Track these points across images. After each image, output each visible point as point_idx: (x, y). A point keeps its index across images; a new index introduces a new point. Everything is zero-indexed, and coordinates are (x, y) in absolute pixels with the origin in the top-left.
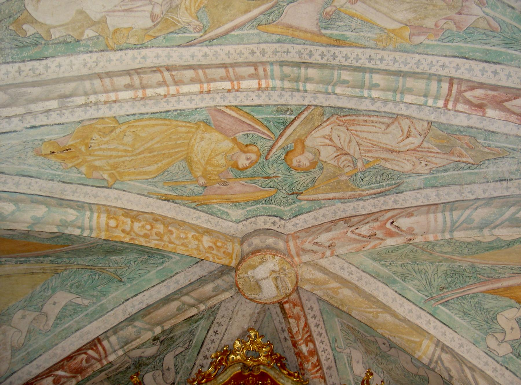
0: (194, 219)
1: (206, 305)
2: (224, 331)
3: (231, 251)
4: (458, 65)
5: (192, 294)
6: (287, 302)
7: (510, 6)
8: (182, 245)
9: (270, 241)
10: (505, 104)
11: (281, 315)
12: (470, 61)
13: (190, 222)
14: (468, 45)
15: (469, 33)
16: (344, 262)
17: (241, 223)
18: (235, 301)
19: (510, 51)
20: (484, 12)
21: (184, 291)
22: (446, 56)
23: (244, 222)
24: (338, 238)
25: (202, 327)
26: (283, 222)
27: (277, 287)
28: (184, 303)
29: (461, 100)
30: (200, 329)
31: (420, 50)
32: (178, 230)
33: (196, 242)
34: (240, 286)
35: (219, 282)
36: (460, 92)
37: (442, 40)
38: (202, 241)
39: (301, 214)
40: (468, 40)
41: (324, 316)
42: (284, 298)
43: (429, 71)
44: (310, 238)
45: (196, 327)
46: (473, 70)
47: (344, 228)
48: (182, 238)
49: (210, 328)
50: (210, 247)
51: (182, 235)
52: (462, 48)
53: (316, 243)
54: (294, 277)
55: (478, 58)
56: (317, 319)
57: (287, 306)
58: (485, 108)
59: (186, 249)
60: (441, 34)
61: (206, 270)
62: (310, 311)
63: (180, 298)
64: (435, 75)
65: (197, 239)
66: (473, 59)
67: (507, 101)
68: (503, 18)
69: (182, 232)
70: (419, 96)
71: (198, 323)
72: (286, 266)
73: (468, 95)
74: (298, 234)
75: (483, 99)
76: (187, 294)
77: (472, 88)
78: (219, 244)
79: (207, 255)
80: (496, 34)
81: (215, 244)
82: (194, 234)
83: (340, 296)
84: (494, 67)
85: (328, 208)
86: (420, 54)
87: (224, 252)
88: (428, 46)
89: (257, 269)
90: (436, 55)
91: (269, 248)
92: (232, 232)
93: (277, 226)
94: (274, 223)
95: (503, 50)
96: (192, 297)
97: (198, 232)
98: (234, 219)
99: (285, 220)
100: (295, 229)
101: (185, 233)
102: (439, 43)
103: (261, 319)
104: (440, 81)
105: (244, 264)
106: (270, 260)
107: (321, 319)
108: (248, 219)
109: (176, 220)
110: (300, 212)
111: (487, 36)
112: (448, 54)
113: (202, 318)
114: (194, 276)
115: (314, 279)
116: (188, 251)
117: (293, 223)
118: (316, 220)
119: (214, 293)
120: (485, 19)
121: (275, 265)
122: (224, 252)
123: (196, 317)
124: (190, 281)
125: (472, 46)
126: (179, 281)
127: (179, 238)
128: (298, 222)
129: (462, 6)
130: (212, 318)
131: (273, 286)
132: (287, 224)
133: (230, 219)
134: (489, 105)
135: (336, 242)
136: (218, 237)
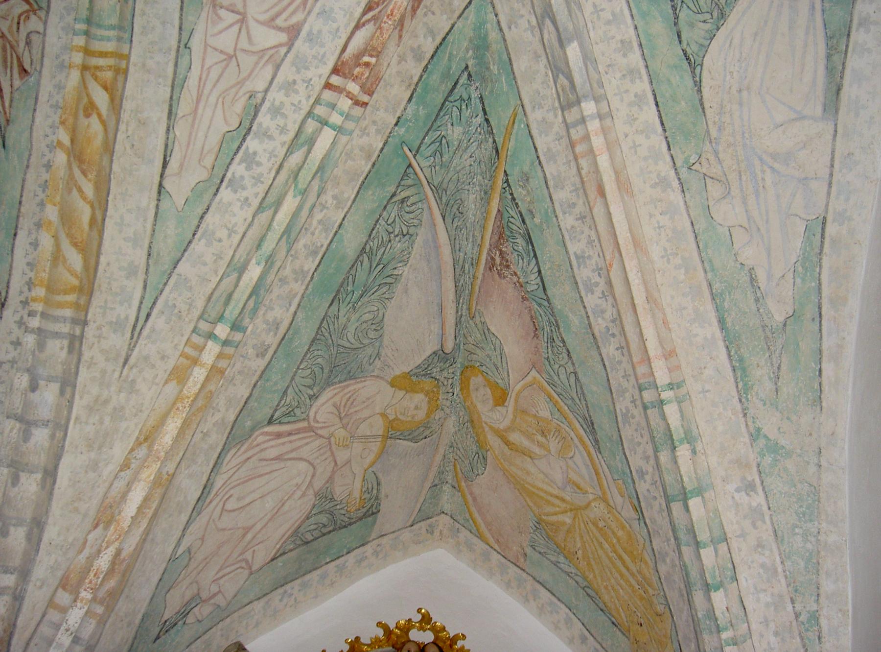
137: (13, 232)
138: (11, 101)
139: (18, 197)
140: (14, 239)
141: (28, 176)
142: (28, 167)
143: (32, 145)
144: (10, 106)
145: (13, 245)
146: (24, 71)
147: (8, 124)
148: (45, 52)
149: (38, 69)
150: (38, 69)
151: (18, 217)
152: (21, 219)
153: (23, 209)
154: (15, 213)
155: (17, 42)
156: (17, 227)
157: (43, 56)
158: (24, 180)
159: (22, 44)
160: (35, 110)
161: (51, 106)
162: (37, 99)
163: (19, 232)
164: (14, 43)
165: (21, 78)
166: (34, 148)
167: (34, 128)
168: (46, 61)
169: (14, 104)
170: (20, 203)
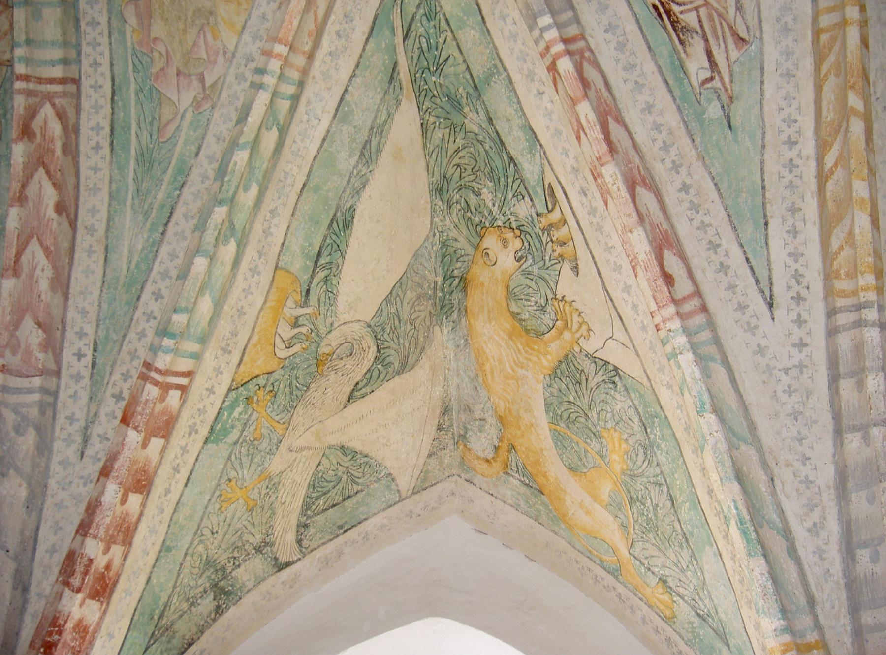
4: (101, 87)
7: (199, 148)
10: (41, 171)
12: (109, 106)
14: (133, 96)
15: (151, 94)
19: (132, 163)
20: (185, 111)
22: (112, 65)
29: (31, 101)
31: (115, 23)
36: (49, 97)
37: (134, 53)
40: (141, 96)
43: (84, 43)
46: (97, 112)
52: (128, 89)
55: (116, 116)
58: (25, 139)
60: (143, 50)
64: (79, 54)
66: (113, 109)
67: (48, 172)
68: (180, 143)
70: (27, 33)
73: (47, 111)
75: (43, 136)
77: (61, 115)
80: (155, 137)
84: (106, 144)
86: (109, 22)
88: (122, 33)
90: (111, 49)
95: (133, 152)
102: (130, 51)
104: (65, 62)
111: (151, 124)
112: (116, 68)
120: (176, 114)
125: (133, 103)
129: (190, 75)
134: (33, 147)
137: (762, 221)
138: (731, 75)
139: (760, 182)
140: (766, 230)
141: (766, 157)
142: (763, 147)
143: (763, 122)
144: (731, 82)
145: (767, 235)
146: (741, 41)
147: (732, 102)
148: (762, 16)
149: (758, 35)
150: (758, 35)
151: (764, 204)
152: (768, 206)
153: (767, 195)
154: (759, 200)
155: (725, 8)
156: (765, 216)
157: (760, 22)
158: (762, 163)
159: (732, 11)
160: (762, 82)
161: (781, 75)
162: (762, 69)
163: (770, 221)
164: (721, 10)
165: (739, 48)
166: (767, 125)
167: (765, 102)
168: (766, 27)
169: (736, 78)
170: (763, 188)
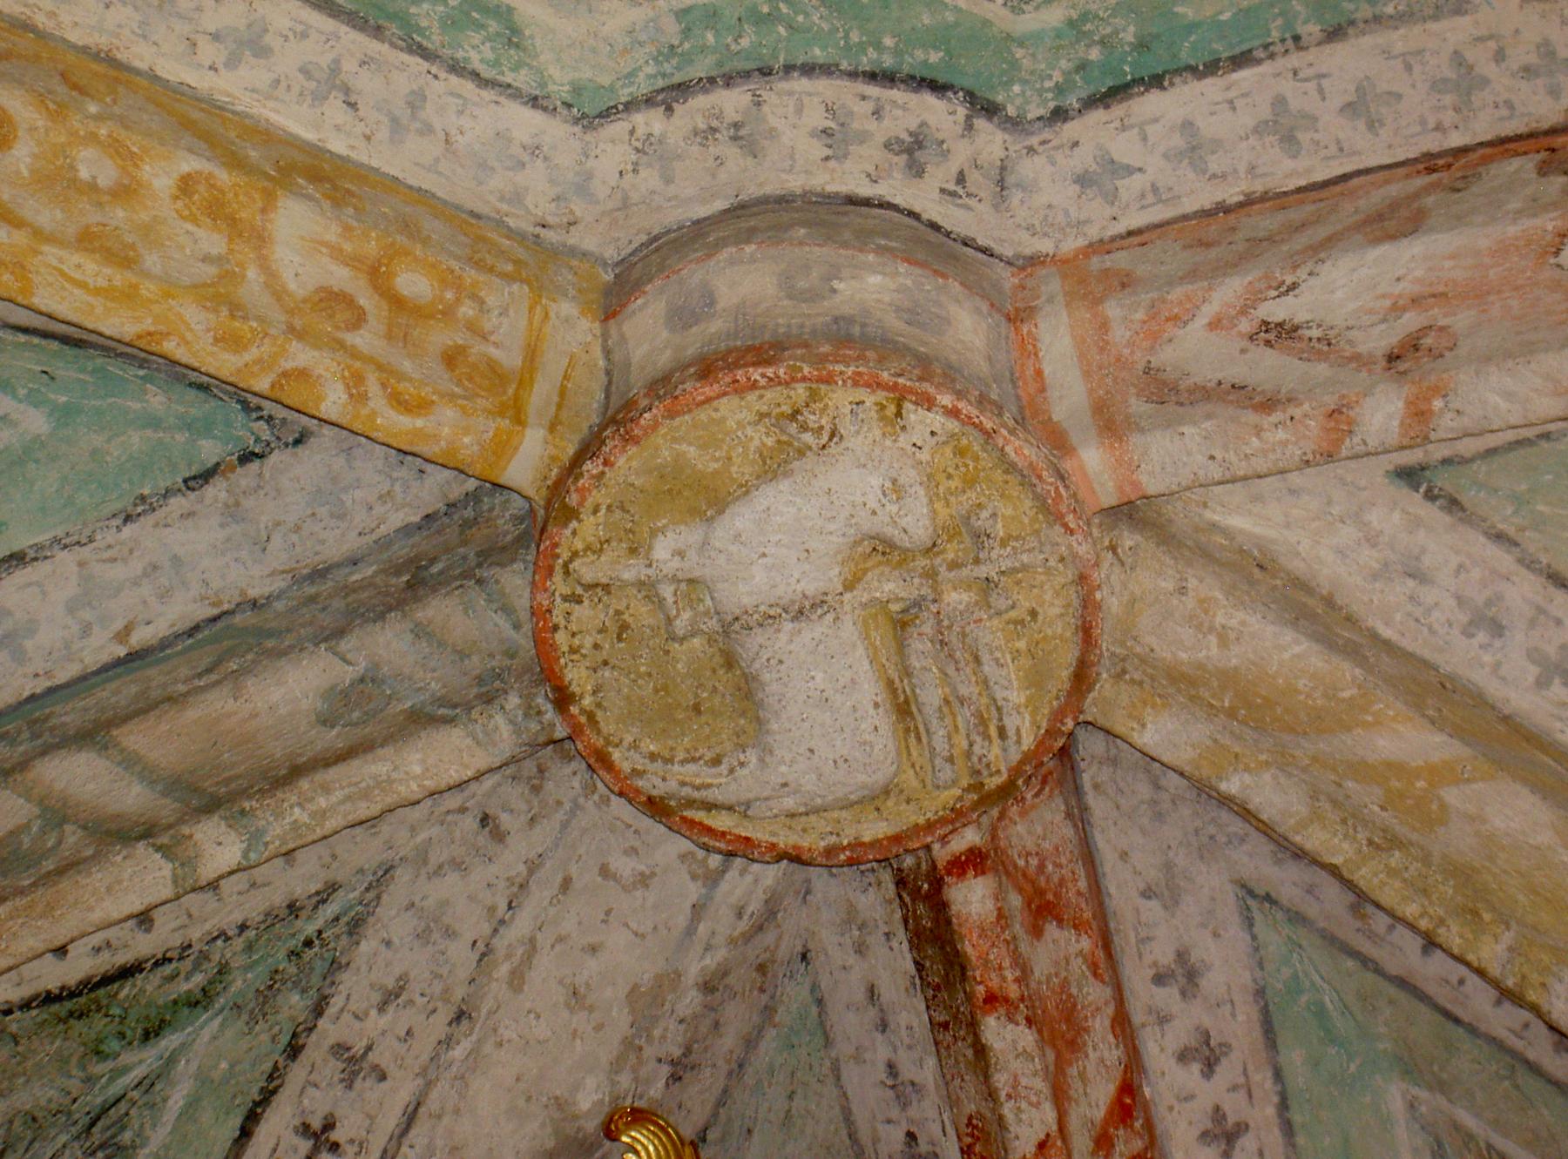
0: (209, 52)
1: (255, 837)
2: (390, 1121)
3: (510, 359)
5: (134, 738)
6: (972, 862)
8: (87, 240)
9: (873, 287)
11: (911, 1014)
13: (172, 70)
16: (1503, 559)
17: (618, 128)
18: (511, 859)
21: (70, 715)
23: (650, 122)
24: (1477, 294)
25: (202, 1078)
26: (991, 141)
27: (904, 710)
28: (56, 813)
30: (177, 1099)
32: (58, 114)
33: (213, 241)
34: (576, 676)
35: (387, 644)
38: (261, 240)
39: (1156, 81)
41: (1294, 1058)
42: (956, 817)
44: (1230, 290)
45: (147, 1084)
47: (1536, 206)
48: (93, 187)
49: (267, 1096)
50: (331, 300)
51: (92, 166)
53: (1280, 334)
54: (1056, 611)
56: (1227, 1072)
57: (972, 899)
59: (120, 278)
61: (279, 555)
62: (1167, 997)
63: (23, 765)
65: (217, 212)
69: (92, 138)
71: (169, 1041)
72: (1007, 511)
74: (1120, 260)
76: (93, 735)
78: (413, 283)
79: (301, 356)
81: (378, 276)
82: (189, 164)
83: (1457, 840)
85: (1399, 39)
87: (451, 358)
89: (741, 518)
91: (850, 343)
92: (537, 194)
93: (939, 175)
94: (913, 150)
96: (131, 762)
97: (235, 162)
98: (560, 83)
99: (1016, 124)
100: (1101, 220)
101: (115, 148)
103: (728, 1041)
105: (627, 466)
106: (863, 437)
107: (1263, 1079)
108: (683, 89)
109: (41, 35)
110: (1153, 63)
113: (199, 1001)
114: (164, 595)
115: (1228, 678)
116: (129, 296)
117: (1083, 159)
118: (1289, 140)
119: (333, 738)
121: (896, 490)
122: (451, 358)
123: (148, 984)
124: (123, 635)
126: (31, 628)
127: (57, 180)
128: (1124, 148)
130: (294, 1004)
131: (870, 689)
132: (1028, 168)
133: (522, 79)
135: (1461, 320)
136: (408, 227)
